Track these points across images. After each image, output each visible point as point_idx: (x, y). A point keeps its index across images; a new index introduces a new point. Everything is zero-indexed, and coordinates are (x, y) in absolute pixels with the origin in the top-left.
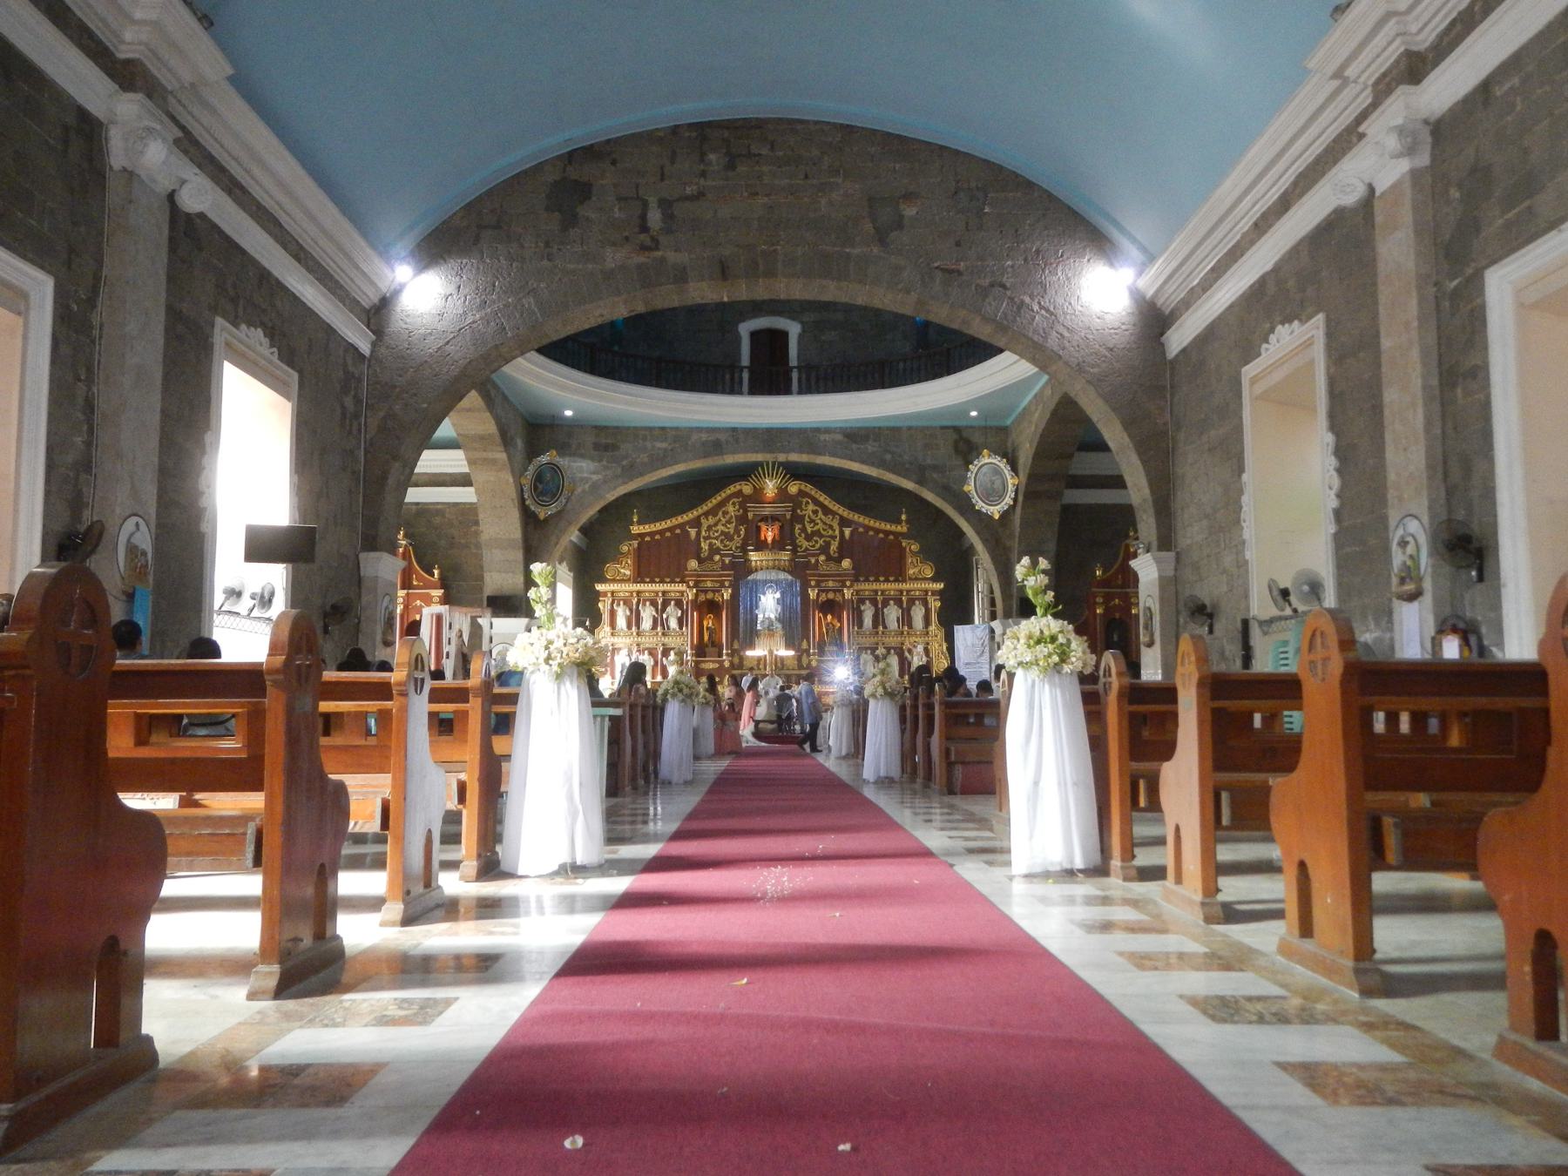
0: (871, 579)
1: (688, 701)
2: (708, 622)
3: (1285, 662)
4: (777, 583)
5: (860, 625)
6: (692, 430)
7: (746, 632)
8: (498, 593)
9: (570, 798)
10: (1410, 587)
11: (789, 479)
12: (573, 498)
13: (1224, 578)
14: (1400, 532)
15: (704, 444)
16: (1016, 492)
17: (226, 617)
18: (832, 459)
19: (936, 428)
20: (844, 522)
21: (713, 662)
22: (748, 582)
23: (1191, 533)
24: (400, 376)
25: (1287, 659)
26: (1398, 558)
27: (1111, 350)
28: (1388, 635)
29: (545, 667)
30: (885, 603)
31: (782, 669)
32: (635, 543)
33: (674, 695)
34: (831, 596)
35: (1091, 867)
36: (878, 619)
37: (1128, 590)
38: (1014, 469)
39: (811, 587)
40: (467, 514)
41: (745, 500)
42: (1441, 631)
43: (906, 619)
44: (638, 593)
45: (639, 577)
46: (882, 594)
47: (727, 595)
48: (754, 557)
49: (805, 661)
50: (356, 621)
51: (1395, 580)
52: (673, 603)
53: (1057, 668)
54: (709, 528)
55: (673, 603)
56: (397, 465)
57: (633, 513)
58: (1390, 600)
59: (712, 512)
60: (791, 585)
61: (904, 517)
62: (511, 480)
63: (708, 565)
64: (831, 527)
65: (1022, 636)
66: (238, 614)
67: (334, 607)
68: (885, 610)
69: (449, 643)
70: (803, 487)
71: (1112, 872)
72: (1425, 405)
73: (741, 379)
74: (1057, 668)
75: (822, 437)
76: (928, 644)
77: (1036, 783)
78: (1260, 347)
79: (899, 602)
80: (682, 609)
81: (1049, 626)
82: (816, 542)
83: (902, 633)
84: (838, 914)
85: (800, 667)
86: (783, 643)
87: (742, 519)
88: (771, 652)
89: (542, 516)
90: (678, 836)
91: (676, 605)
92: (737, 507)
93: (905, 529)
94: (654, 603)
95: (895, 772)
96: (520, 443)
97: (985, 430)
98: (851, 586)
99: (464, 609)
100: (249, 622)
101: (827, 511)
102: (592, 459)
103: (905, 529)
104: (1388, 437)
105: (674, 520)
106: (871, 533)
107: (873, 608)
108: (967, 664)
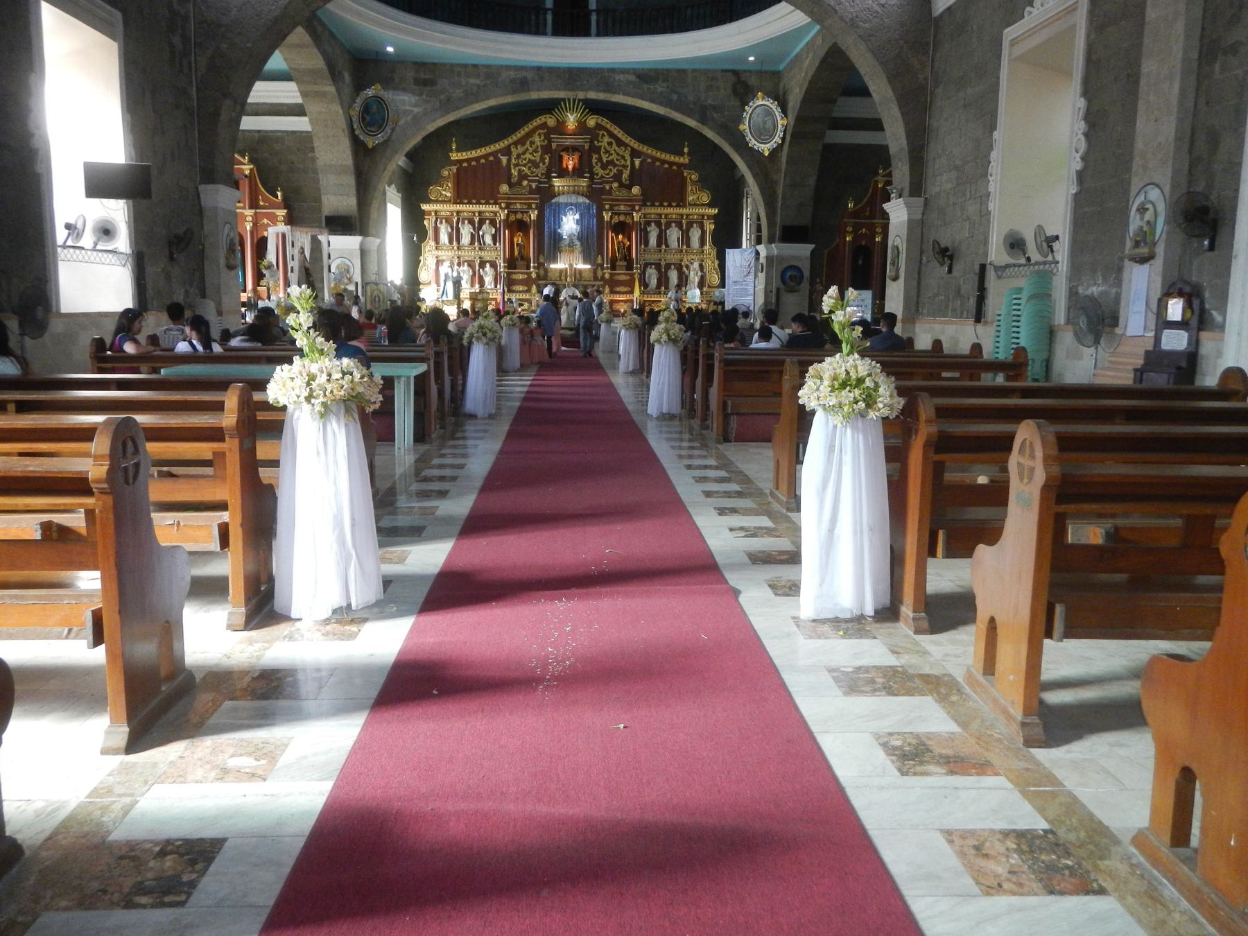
0: (657, 204)
1: (492, 343)
2: (518, 239)
3: (1018, 307)
4: (577, 205)
5: (647, 244)
7: (552, 245)
8: (336, 214)
9: (342, 542)
10: (1144, 250)
11: (587, 114)
12: (398, 129)
13: (967, 224)
14: (1141, 198)
15: (513, 81)
17: (72, 250)
18: (626, 98)
19: (717, 70)
20: (635, 154)
21: (523, 273)
22: (551, 205)
23: (941, 182)
24: (224, 15)
25: (1019, 304)
26: (1135, 223)
27: (883, 6)
28: (1114, 290)
29: (306, 407)
30: (668, 225)
31: (580, 280)
32: (454, 169)
33: (478, 339)
34: (622, 218)
35: (880, 607)
36: (662, 239)
37: (874, 221)
38: (784, 111)
39: (606, 210)
40: (303, 141)
41: (549, 132)
42: (1167, 294)
43: (685, 239)
44: (458, 212)
45: (458, 199)
46: (666, 218)
47: (534, 215)
48: (557, 182)
49: (599, 274)
50: (201, 247)
51: (1129, 244)
52: (487, 221)
53: (863, 415)
54: (518, 156)
55: (487, 221)
56: (228, 102)
58: (1122, 259)
59: (521, 142)
60: (588, 207)
61: (686, 150)
62: (341, 111)
63: (517, 189)
64: (623, 157)
65: (827, 376)
66: (82, 248)
67: (177, 236)
68: (668, 231)
69: (293, 259)
70: (599, 121)
71: (901, 618)
72: (1182, 79)
73: (545, 20)
74: (863, 415)
75: (617, 77)
76: (703, 261)
77: (831, 530)
78: (1024, 9)
79: (680, 225)
80: (495, 227)
81: (856, 367)
82: (611, 170)
83: (682, 251)
84: (622, 726)
85: (596, 278)
86: (581, 260)
87: (547, 149)
88: (571, 266)
89: (370, 146)
90: (475, 525)
91: (490, 223)
92: (542, 138)
93: (687, 161)
94: (471, 222)
95: (676, 409)
97: (760, 73)
98: (639, 210)
99: (304, 229)
100: (95, 253)
101: (620, 143)
102: (413, 93)
103: (687, 161)
104: (1141, 106)
105: (488, 149)
106: (658, 164)
107: (658, 230)
108: (735, 282)
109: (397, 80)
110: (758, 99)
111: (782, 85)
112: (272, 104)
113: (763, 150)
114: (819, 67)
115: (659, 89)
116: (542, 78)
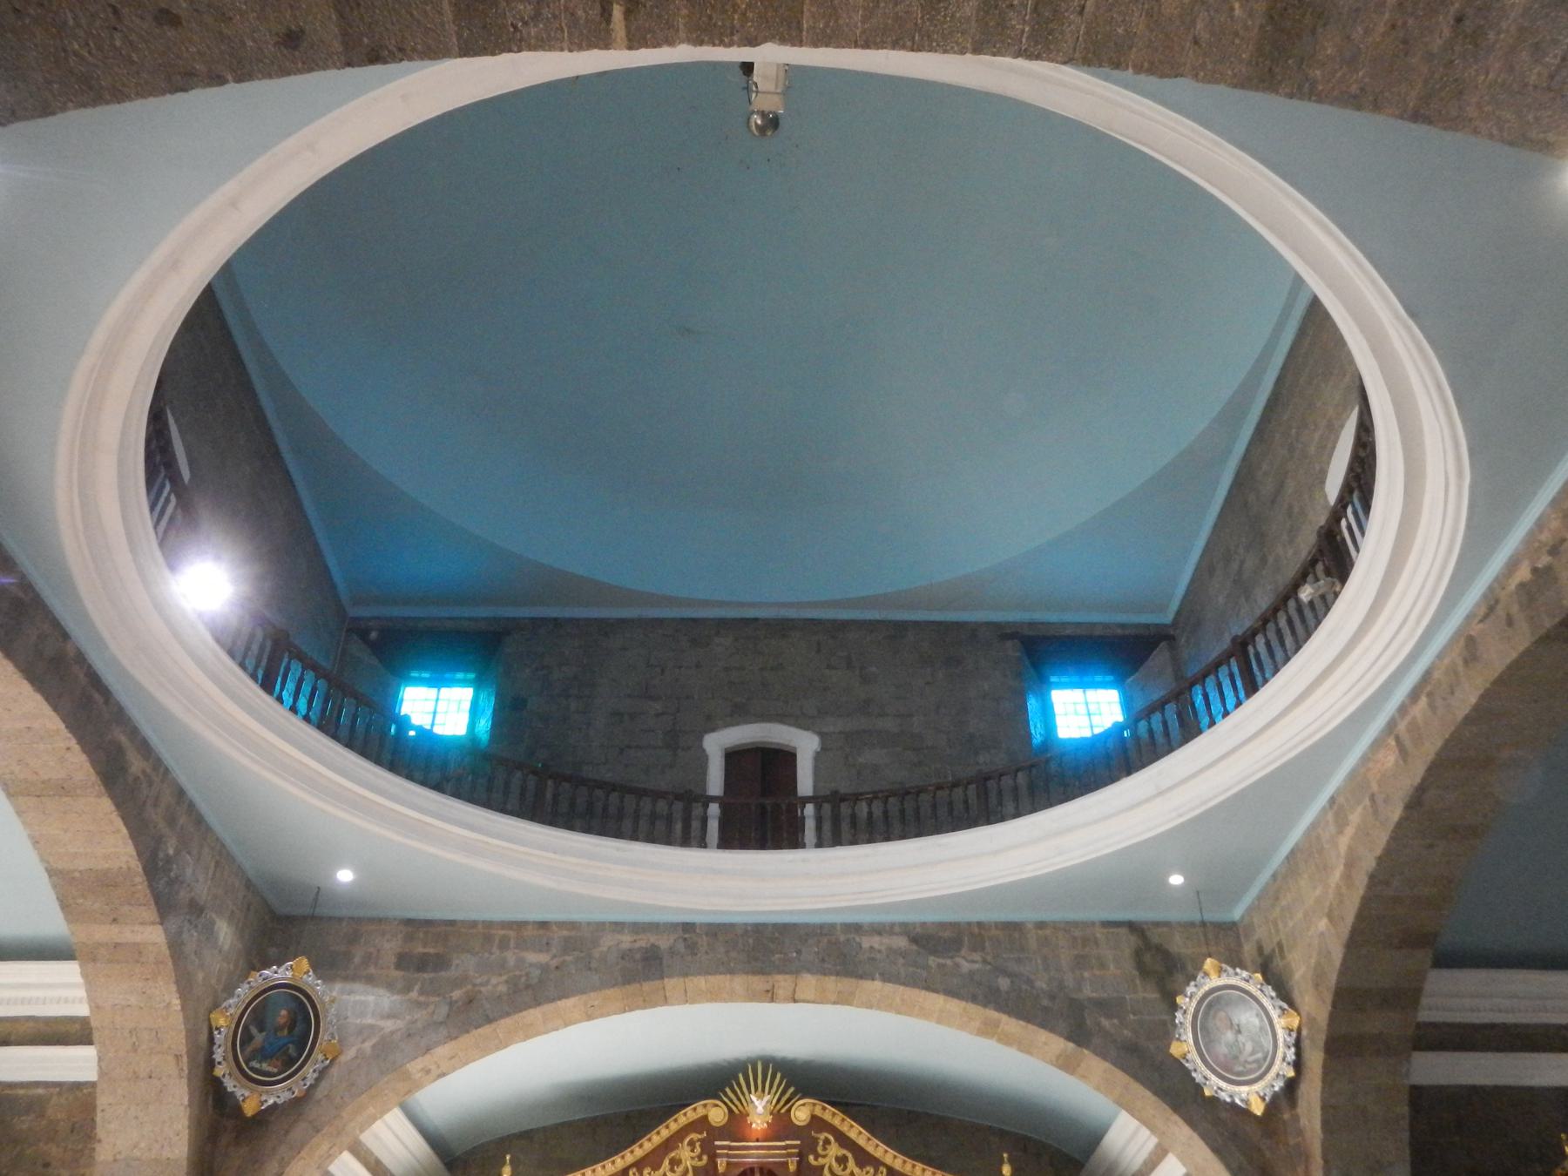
6: (601, 926)
12: (334, 1071)
15: (625, 955)
16: (1298, 1045)
19: (1093, 924)
38: (1285, 995)
40: (80, 1096)
57: (504, 1164)
62: (176, 1002)
70: (818, 1112)
73: (704, 821)
75: (866, 942)
89: (249, 1109)
92: (698, 1150)
96: (225, 932)
101: (864, 1158)
102: (390, 986)
109: (357, 960)
110: (1206, 974)
111: (1248, 949)
112: (48, 1021)
113: (1247, 1102)
114: (1399, 825)
115: (966, 966)
116: (692, 948)
